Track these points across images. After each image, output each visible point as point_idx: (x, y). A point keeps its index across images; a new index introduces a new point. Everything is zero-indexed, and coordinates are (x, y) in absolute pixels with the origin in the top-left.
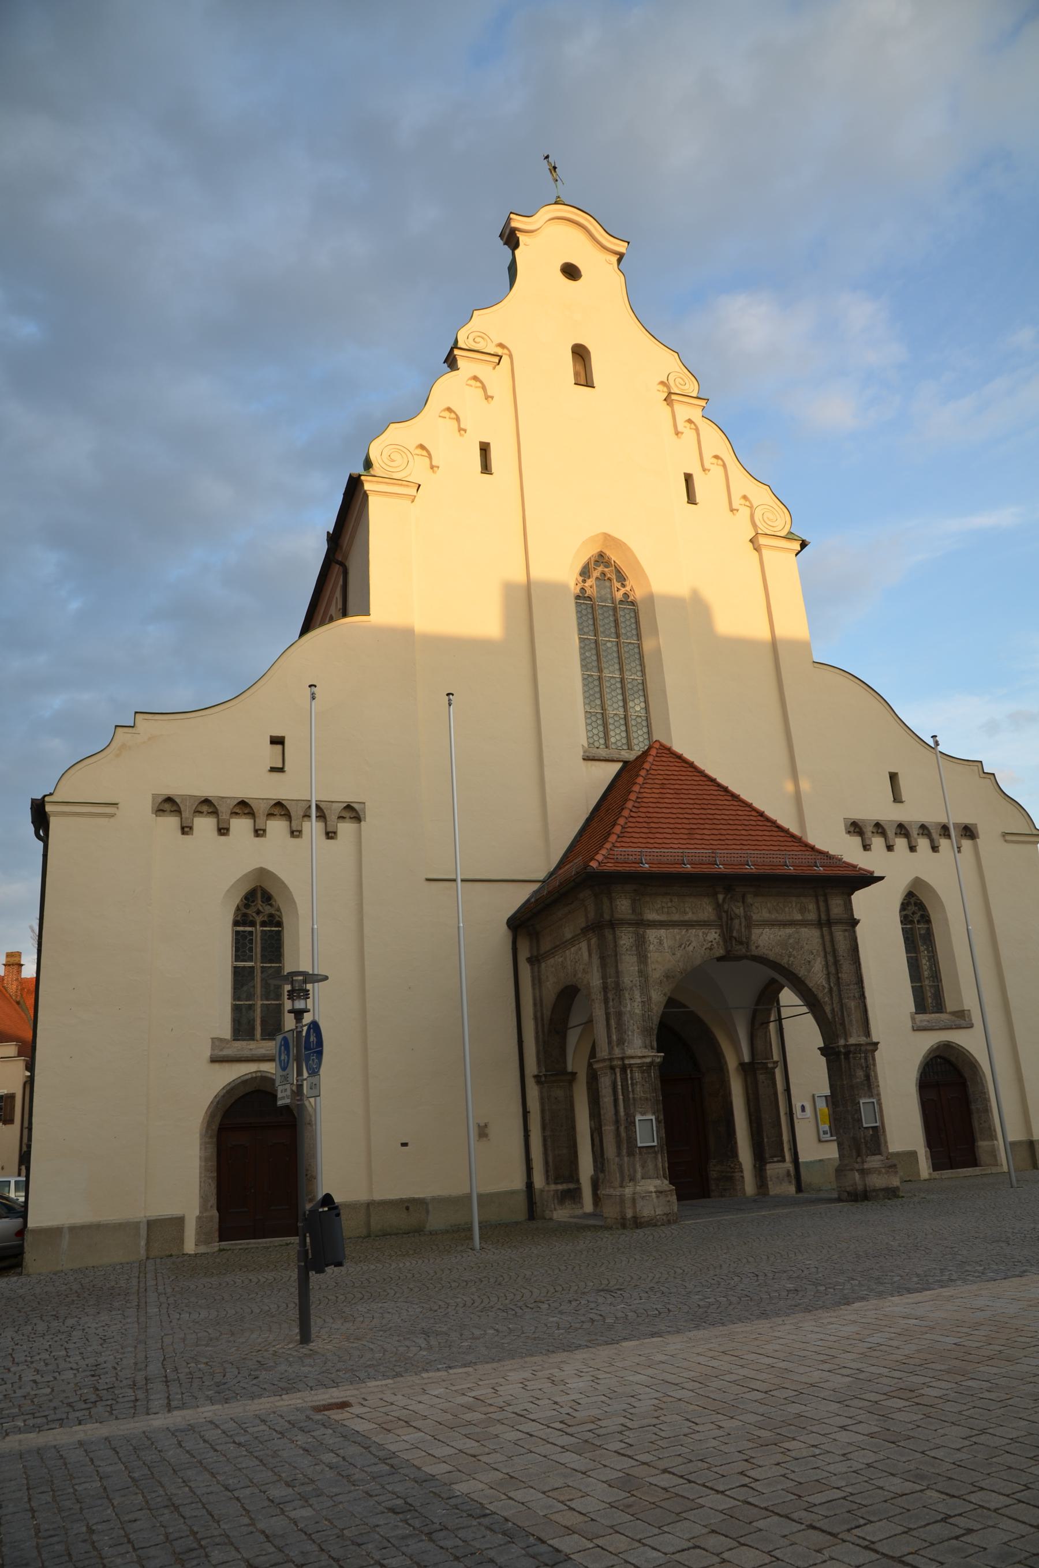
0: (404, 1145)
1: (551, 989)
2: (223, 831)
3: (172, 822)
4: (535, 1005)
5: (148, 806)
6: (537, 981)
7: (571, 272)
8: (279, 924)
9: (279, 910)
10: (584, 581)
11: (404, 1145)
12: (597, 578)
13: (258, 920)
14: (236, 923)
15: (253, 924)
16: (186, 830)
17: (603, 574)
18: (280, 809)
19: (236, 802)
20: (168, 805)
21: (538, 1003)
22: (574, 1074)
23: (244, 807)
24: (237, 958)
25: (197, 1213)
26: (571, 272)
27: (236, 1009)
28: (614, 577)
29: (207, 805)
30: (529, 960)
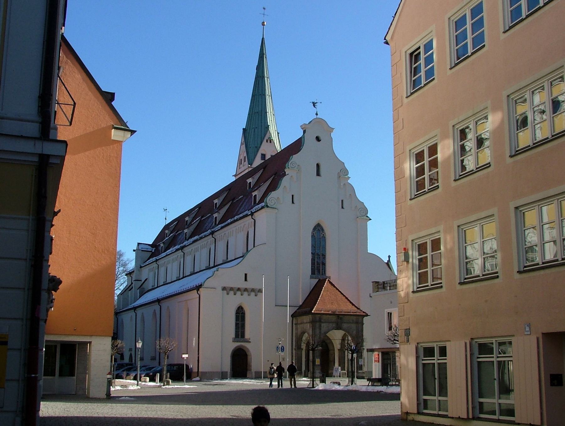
0: (268, 361)
1: (300, 331)
2: (235, 294)
3: (225, 292)
4: (296, 334)
5: (221, 289)
6: (297, 329)
7: (318, 139)
8: (244, 314)
9: (245, 311)
10: (314, 231)
11: (268, 361)
12: (317, 231)
13: (241, 313)
14: (236, 314)
15: (239, 314)
16: (228, 294)
17: (318, 229)
18: (246, 290)
19: (237, 288)
20: (224, 289)
21: (296, 334)
22: (303, 349)
23: (239, 289)
24: (236, 321)
25: (229, 371)
26: (318, 139)
27: (236, 331)
28: (321, 230)
29: (232, 289)
30: (295, 324)
